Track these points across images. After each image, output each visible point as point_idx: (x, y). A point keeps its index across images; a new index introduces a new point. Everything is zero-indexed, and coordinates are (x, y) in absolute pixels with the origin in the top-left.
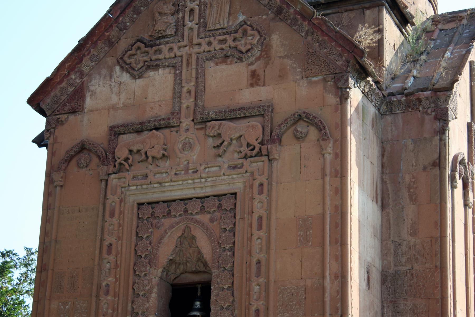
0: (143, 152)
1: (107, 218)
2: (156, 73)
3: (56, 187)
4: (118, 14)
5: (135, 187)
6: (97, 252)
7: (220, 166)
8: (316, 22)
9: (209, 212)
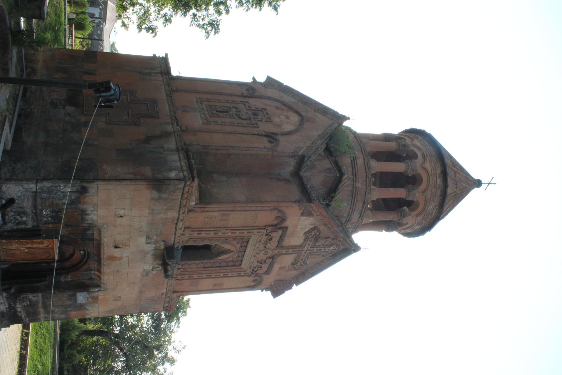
1: (248, 231)
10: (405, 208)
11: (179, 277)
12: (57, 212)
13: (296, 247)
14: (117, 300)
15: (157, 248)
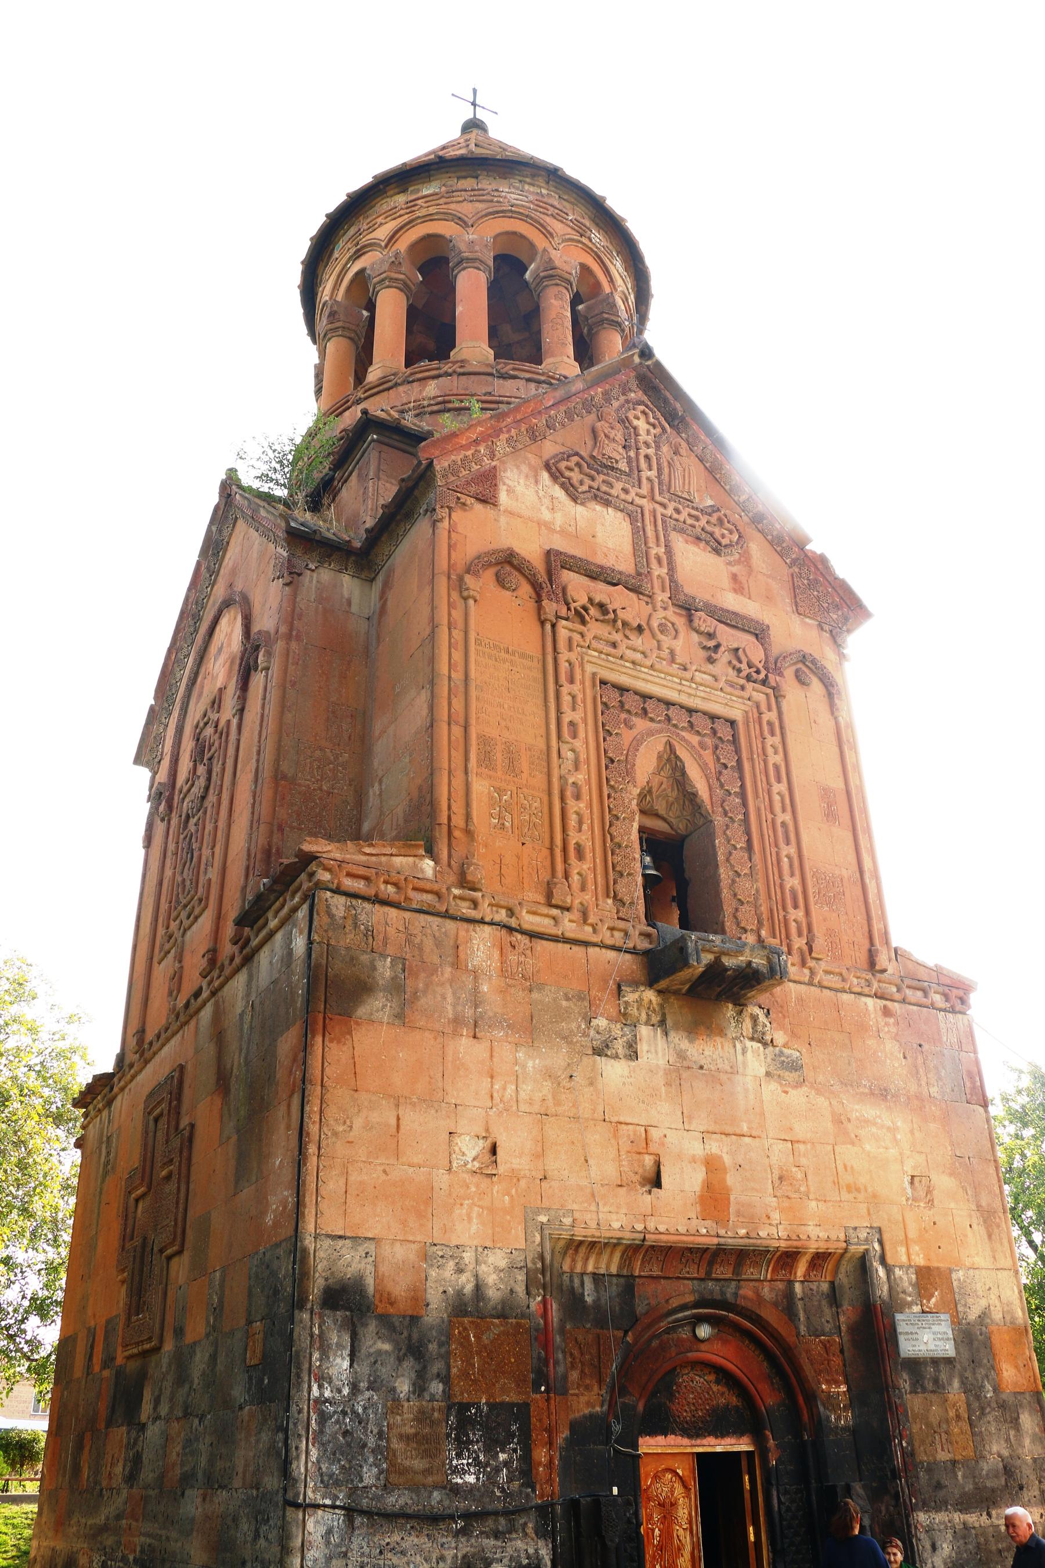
0: (610, 607)
1: (563, 679)
2: (605, 510)
3: (465, 599)
4: (551, 403)
5: (596, 654)
6: (553, 727)
7: (714, 676)
8: (809, 554)
9: (698, 733)
10: (527, 275)
11: (799, 943)
12: (464, 1424)
13: (638, 533)
14: (929, 1192)
15: (655, 1019)
